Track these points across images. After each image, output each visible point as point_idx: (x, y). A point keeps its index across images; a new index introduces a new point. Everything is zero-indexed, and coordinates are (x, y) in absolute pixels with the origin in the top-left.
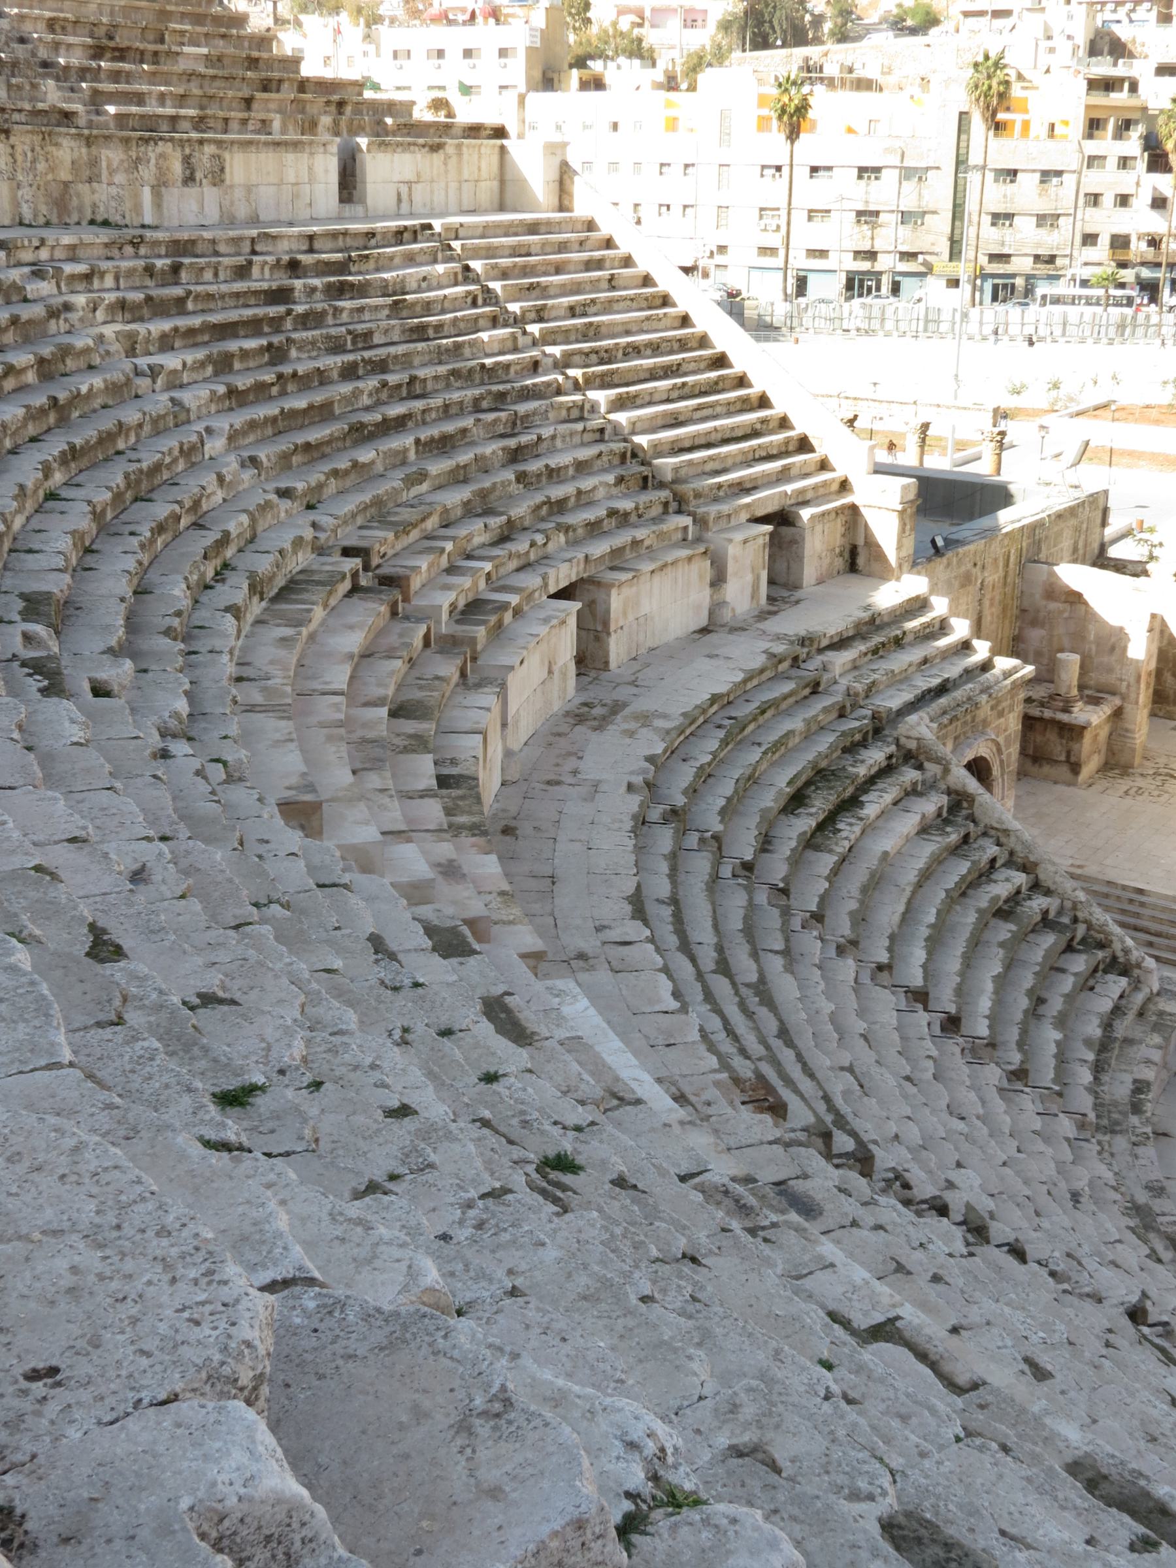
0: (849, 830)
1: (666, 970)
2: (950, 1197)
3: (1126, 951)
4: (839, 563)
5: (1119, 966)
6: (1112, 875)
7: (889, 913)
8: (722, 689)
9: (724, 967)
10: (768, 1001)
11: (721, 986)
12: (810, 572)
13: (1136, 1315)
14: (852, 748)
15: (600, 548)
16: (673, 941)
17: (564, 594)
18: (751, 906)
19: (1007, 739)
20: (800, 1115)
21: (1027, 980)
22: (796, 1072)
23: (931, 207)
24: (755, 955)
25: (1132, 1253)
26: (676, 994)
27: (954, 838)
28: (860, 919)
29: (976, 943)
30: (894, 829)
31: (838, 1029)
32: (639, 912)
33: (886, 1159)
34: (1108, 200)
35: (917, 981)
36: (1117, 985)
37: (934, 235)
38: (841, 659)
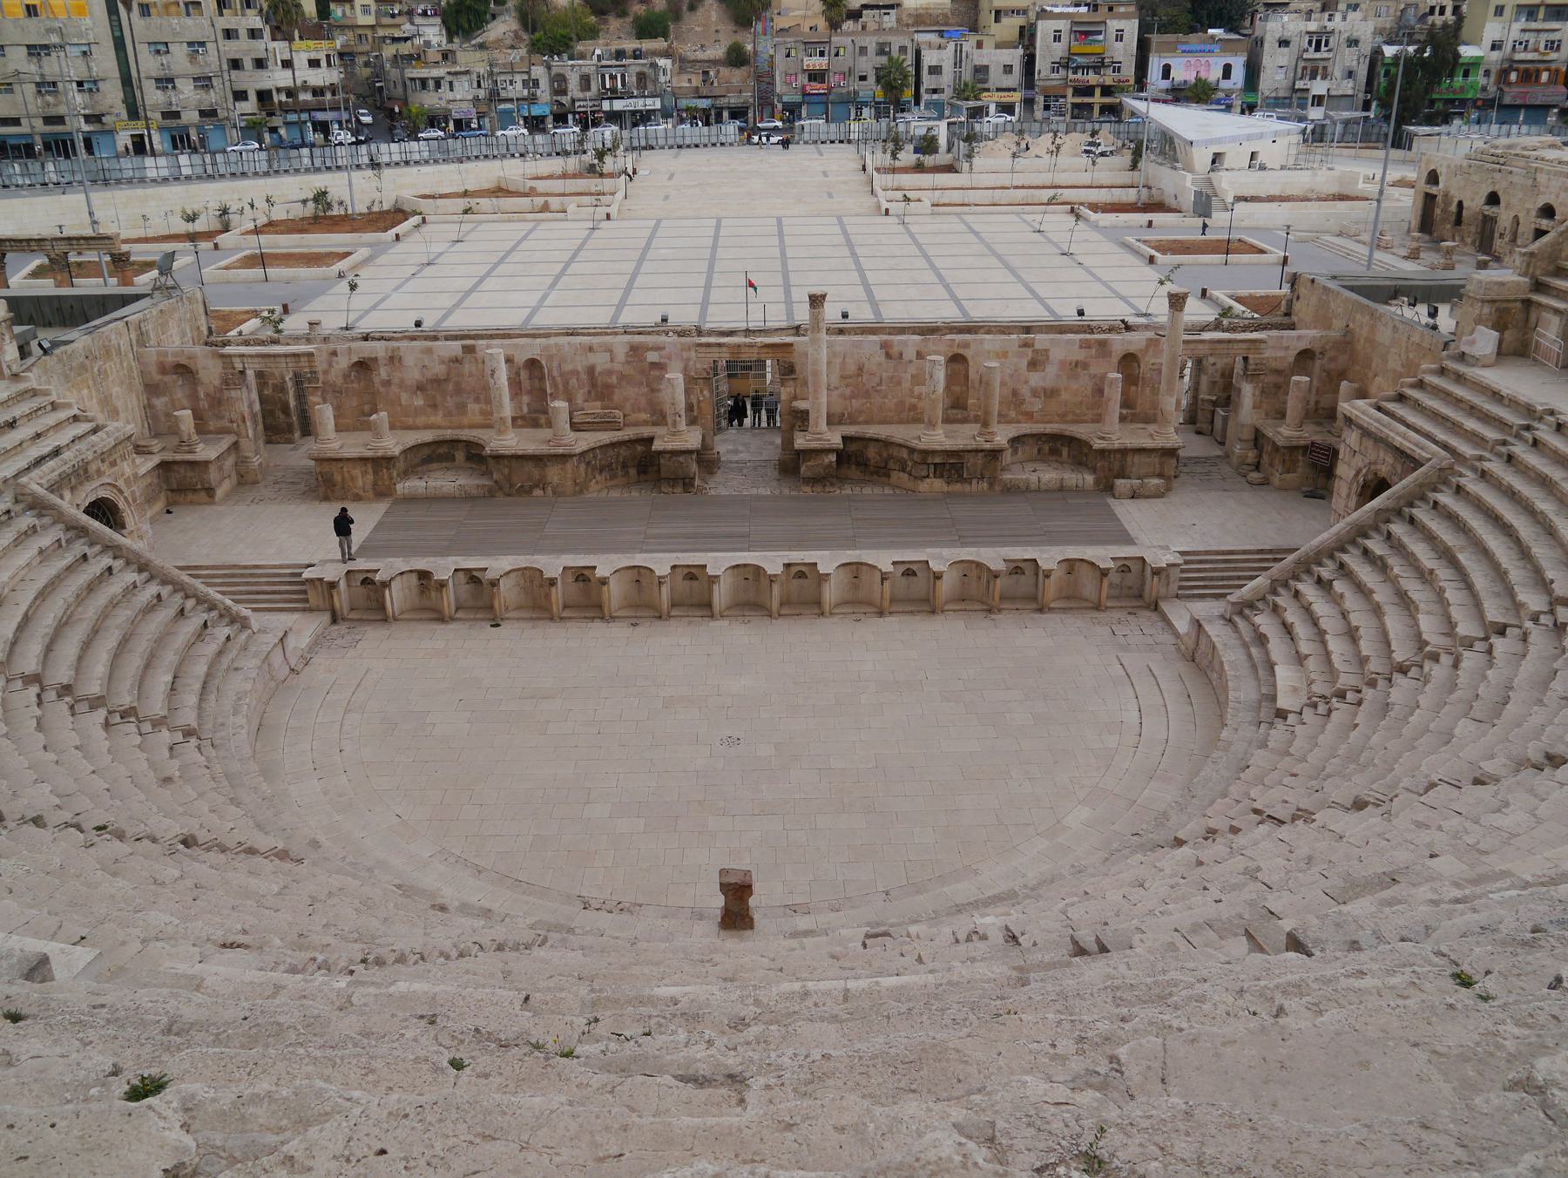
3: (228, 609)
23: (101, 75)
34: (248, 64)
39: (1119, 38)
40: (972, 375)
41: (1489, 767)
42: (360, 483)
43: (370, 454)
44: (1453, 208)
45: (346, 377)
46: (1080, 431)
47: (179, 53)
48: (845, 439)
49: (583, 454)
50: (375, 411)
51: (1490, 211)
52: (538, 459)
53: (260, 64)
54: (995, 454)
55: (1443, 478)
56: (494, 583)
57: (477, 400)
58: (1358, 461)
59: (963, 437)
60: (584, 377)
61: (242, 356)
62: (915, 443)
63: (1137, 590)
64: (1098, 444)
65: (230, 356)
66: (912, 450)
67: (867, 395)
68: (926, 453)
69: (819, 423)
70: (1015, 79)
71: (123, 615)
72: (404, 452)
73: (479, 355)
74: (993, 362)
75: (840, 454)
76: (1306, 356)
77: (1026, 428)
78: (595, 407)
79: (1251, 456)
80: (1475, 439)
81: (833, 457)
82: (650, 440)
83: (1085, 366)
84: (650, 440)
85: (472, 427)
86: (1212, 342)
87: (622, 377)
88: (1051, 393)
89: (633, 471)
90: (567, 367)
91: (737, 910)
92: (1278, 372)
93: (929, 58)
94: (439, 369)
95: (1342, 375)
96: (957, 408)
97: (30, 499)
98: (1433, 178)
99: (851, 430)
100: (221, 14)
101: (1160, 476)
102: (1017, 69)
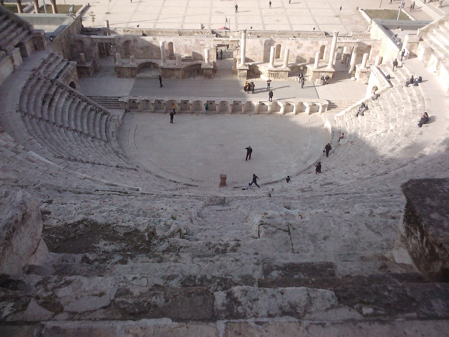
0: (54, 104)
3: (106, 111)
4: (34, 49)
5: (105, 113)
6: (101, 95)
8: (23, 86)
9: (45, 138)
11: (46, 141)
12: (29, 53)
13: (117, 167)
14: (50, 88)
16: (36, 137)
19: (76, 76)
20: (65, 156)
21: (91, 121)
22: (62, 150)
25: (116, 158)
26: (42, 146)
27: (72, 100)
28: (62, 120)
30: (61, 102)
32: (30, 134)
33: (79, 158)
36: (106, 116)
38: (42, 71)
41: (365, 163)
42: (127, 73)
43: (130, 66)
45: (123, 45)
49: (184, 69)
52: (173, 70)
57: (156, 52)
60: (184, 47)
61: (95, 38)
65: (93, 38)
67: (255, 54)
71: (86, 113)
72: (139, 66)
73: (157, 40)
75: (248, 70)
83: (312, 48)
85: (155, 58)
89: (196, 72)
90: (179, 45)
91: (223, 182)
97: (59, 84)
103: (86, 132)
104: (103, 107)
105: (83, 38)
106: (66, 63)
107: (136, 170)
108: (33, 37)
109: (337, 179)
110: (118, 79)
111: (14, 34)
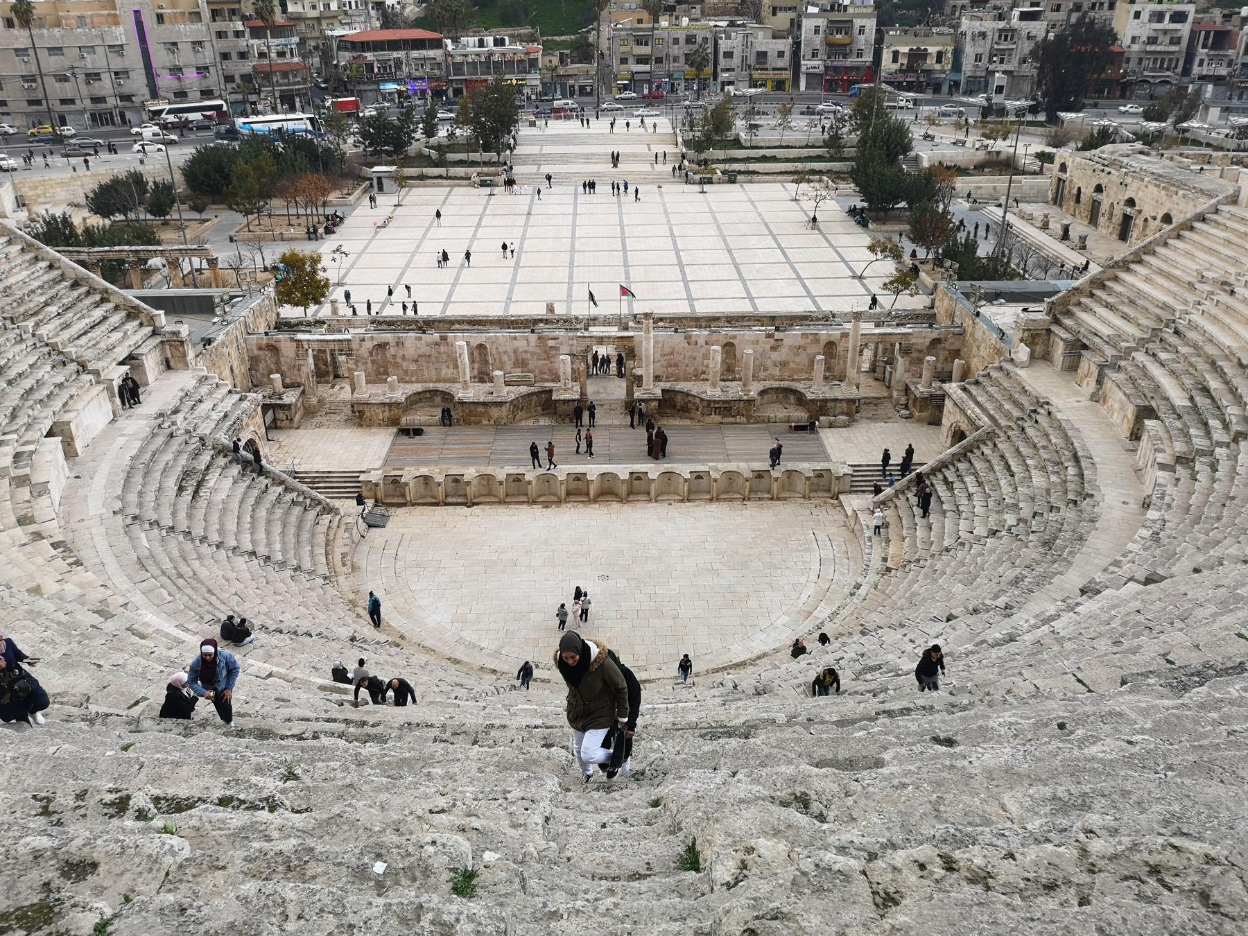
1: (162, 586)
2: (281, 626)
4: (162, 367)
5: (328, 510)
7: (231, 526)
8: (133, 453)
9: (180, 576)
10: (200, 581)
11: (181, 582)
13: (353, 639)
14: (196, 455)
15: (57, 404)
17: (50, 434)
18: (180, 543)
24: (189, 565)
26: (170, 594)
28: (221, 531)
29: (269, 522)
31: (227, 580)
34: (234, 56)
35: (250, 548)
36: (326, 519)
37: (137, 83)
38: (179, 418)
39: (861, 32)
40: (738, 353)
41: (954, 612)
44: (1075, 191)
46: (799, 386)
47: (185, 48)
48: (663, 391)
50: (388, 375)
51: (1097, 196)
52: (484, 404)
53: (243, 55)
54: (750, 402)
55: (990, 436)
56: (468, 483)
58: (952, 419)
59: (734, 390)
62: (703, 396)
63: (826, 488)
64: (810, 396)
66: (702, 400)
68: (709, 401)
69: (648, 383)
70: (785, 62)
74: (750, 342)
76: (936, 342)
77: (768, 384)
78: (517, 373)
79: (903, 401)
80: (1008, 415)
81: (655, 403)
82: (551, 391)
83: (805, 349)
84: (551, 391)
86: (879, 334)
87: (533, 354)
88: (784, 364)
90: (501, 349)
92: (920, 351)
93: (724, 45)
94: (425, 350)
95: (956, 354)
96: (729, 371)
98: (1063, 168)
99: (667, 385)
100: (214, 20)
101: (847, 414)
102: (787, 54)
103: (279, 557)
104: (322, 497)
105: (279, 341)
106: (238, 396)
107: (398, 645)
108: (162, 342)
109: (890, 657)
110: (360, 431)
111: (117, 336)
